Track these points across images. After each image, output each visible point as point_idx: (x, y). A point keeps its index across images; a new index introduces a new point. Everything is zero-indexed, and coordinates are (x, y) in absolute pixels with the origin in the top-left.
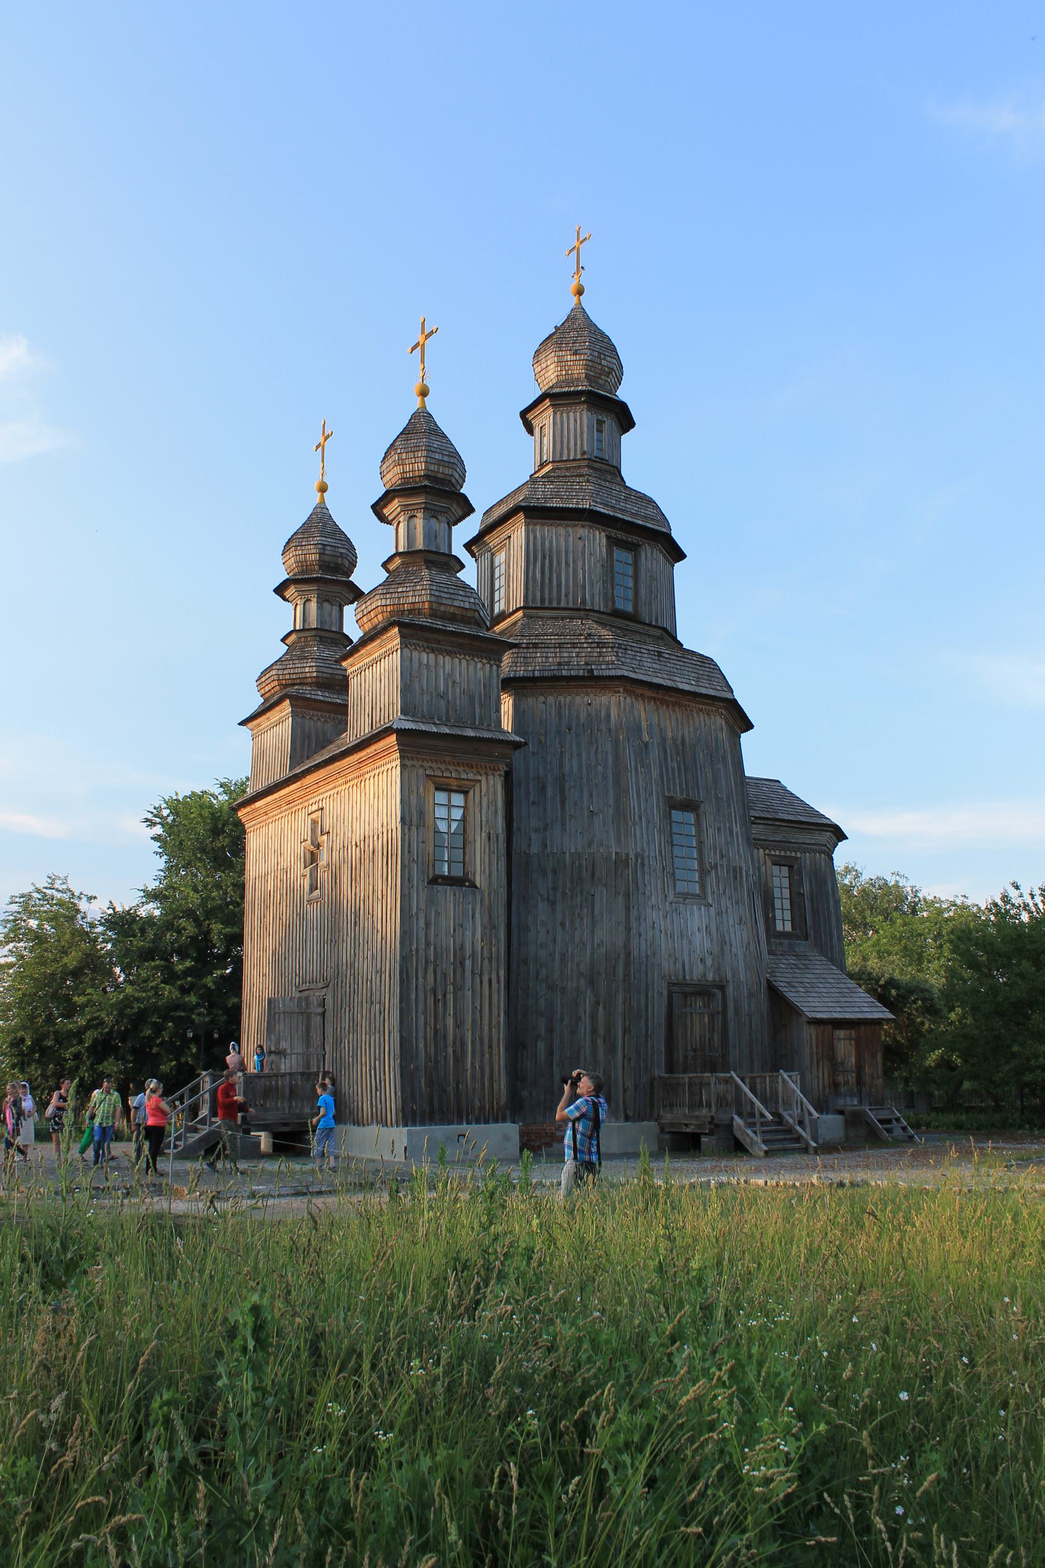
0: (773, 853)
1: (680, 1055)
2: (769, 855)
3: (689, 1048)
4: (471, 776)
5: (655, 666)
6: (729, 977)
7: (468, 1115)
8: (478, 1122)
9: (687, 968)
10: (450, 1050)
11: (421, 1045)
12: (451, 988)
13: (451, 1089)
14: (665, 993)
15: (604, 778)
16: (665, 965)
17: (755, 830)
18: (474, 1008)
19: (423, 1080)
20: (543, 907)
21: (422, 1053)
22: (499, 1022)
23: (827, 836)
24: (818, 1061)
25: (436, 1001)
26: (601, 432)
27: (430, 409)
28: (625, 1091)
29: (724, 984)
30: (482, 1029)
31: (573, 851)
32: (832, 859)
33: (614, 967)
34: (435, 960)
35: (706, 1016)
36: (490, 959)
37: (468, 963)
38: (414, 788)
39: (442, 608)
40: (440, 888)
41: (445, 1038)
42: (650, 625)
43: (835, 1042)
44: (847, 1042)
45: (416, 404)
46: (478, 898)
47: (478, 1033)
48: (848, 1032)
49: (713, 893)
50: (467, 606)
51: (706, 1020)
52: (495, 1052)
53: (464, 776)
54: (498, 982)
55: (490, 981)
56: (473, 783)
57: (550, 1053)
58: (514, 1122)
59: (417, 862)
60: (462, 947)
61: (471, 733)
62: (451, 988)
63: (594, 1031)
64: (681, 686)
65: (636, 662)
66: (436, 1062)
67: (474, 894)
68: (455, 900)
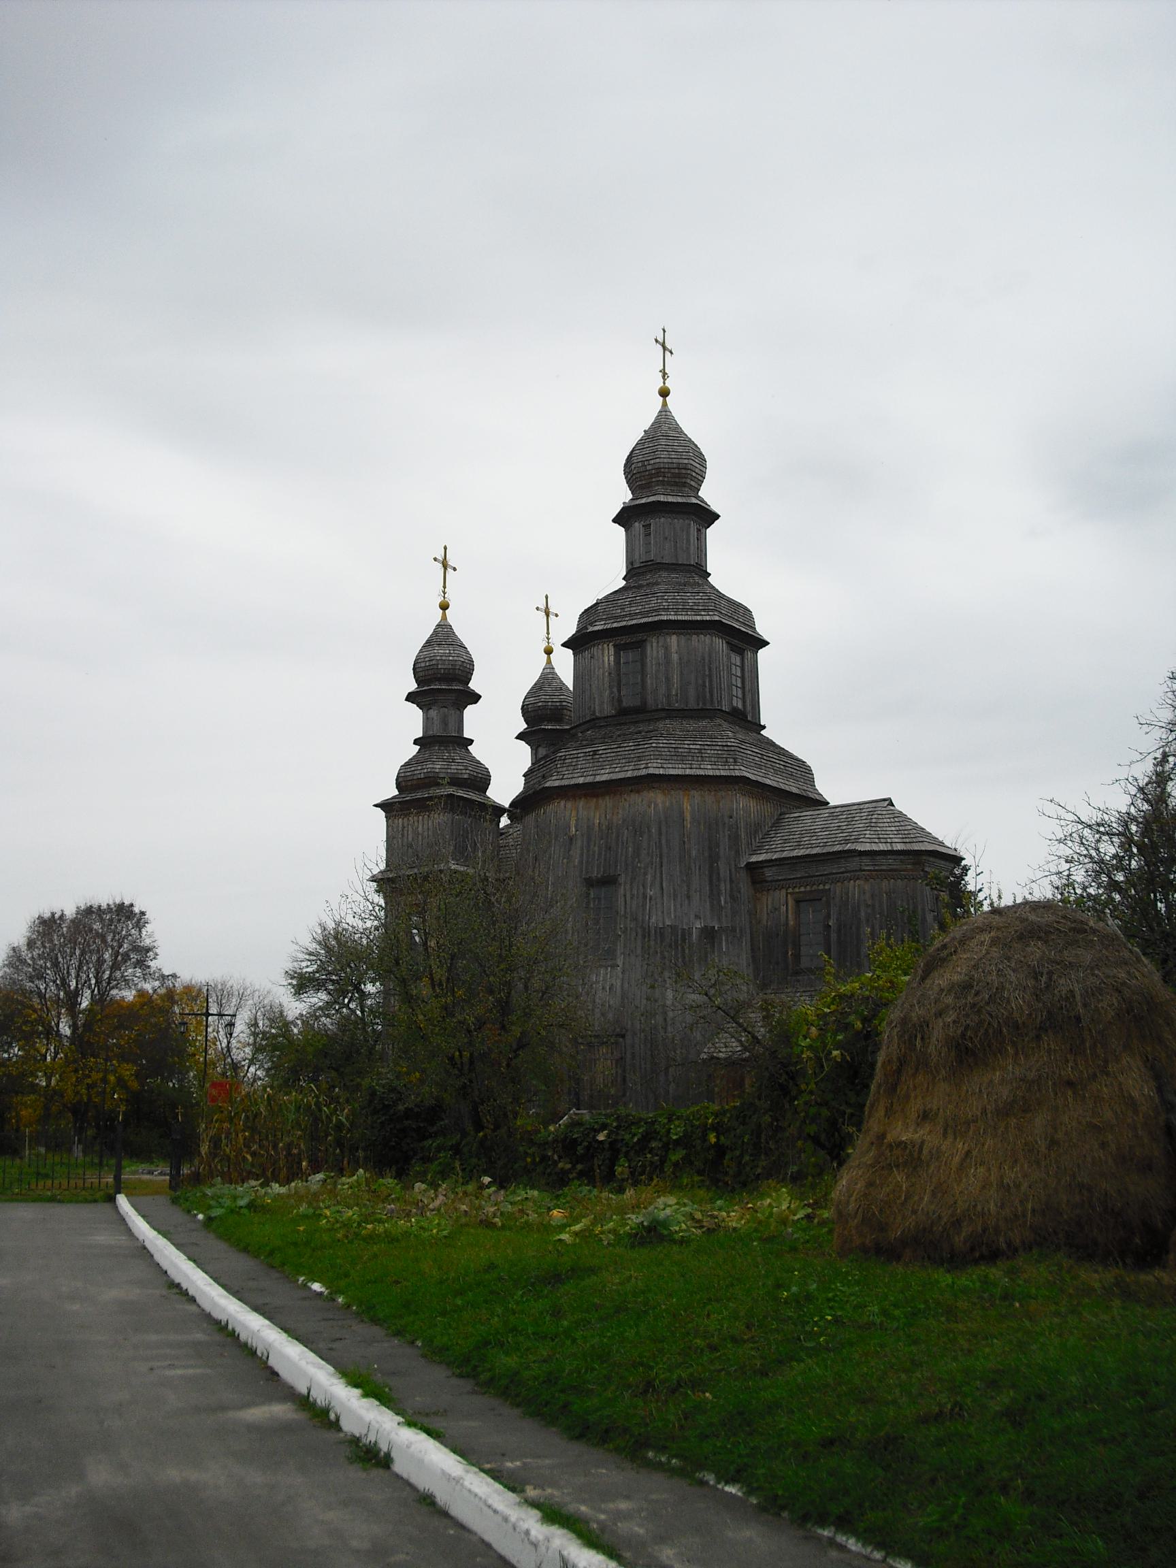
0: (797, 890)
26: (650, 534)
29: (623, 1033)
42: (657, 710)
50: (422, 776)
64: (598, 779)
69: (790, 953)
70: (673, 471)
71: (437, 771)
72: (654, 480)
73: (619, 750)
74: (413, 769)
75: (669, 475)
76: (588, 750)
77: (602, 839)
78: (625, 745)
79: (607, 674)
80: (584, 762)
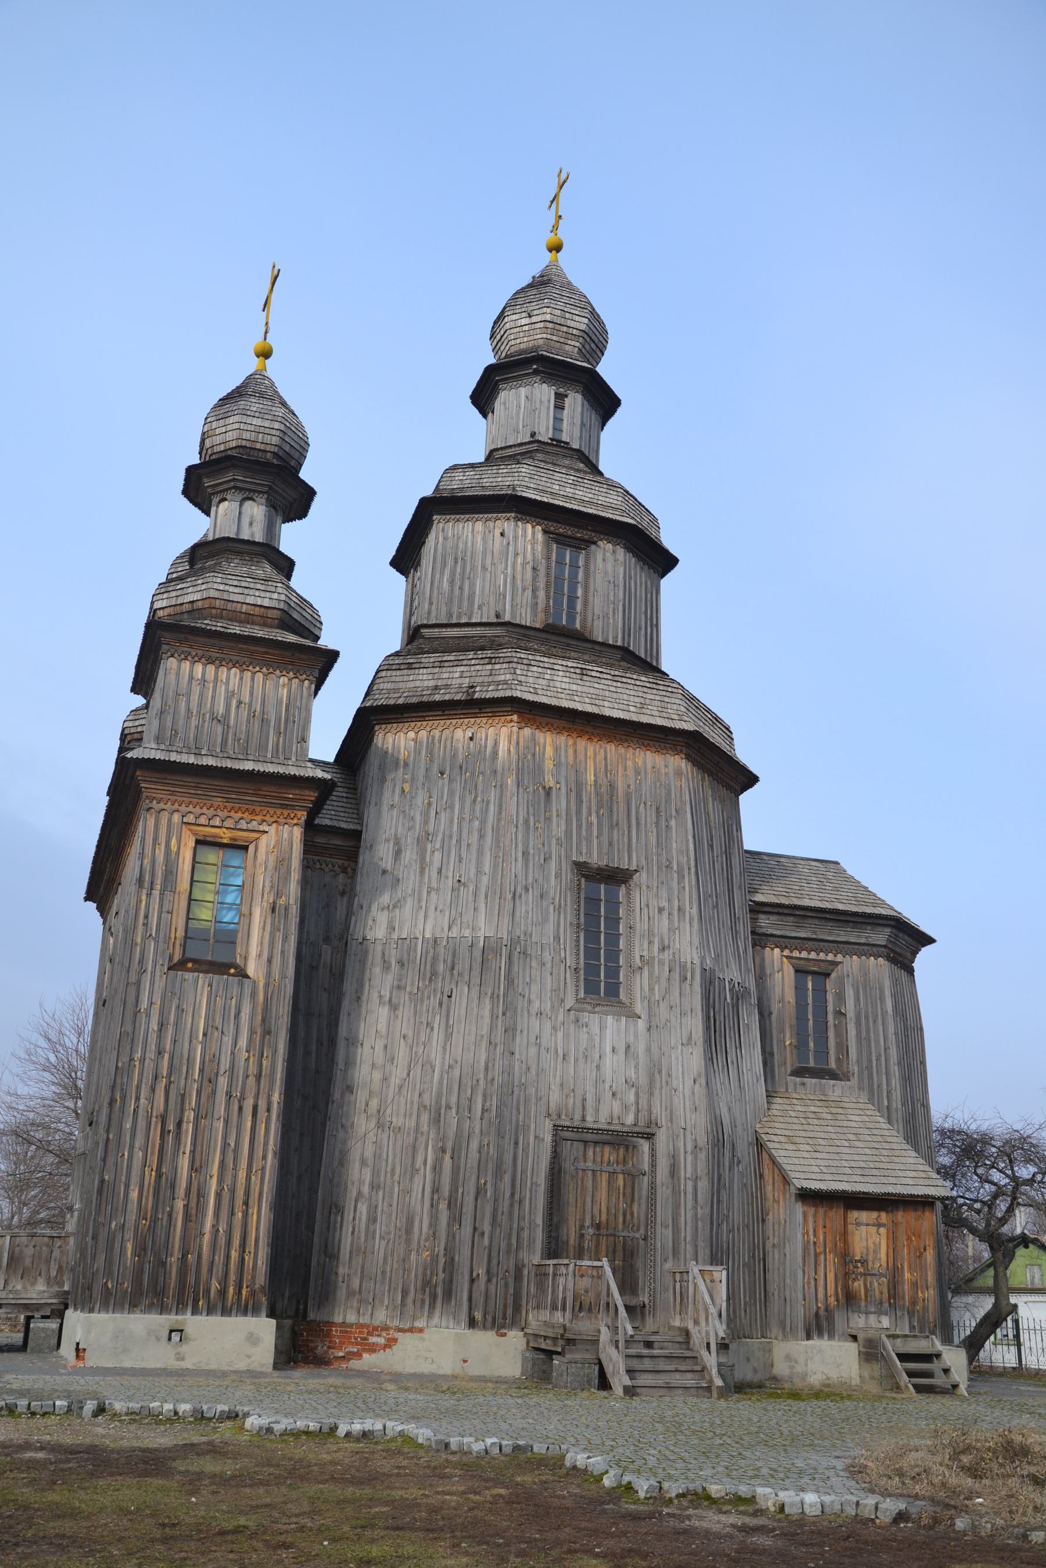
0: (796, 954)
1: (570, 1233)
2: (787, 957)
3: (588, 1223)
4: (254, 825)
5: (574, 687)
6: (663, 1121)
7: (196, 1301)
8: (210, 1311)
9: (590, 1103)
10: (180, 1204)
11: (134, 1195)
12: (190, 1115)
13: (173, 1260)
14: (548, 1138)
15: (482, 837)
16: (555, 1097)
17: (766, 923)
18: (225, 1145)
19: (129, 1246)
20: (384, 1012)
21: (133, 1207)
22: (263, 1169)
23: (881, 937)
24: (816, 1255)
25: (164, 1133)
26: (563, 408)
27: (270, 373)
28: (472, 1281)
30: (235, 1177)
31: (428, 935)
32: (910, 971)
33: (470, 1100)
34: (170, 1075)
35: (621, 1177)
36: (259, 1077)
37: (223, 1082)
38: (163, 840)
39: (229, 606)
40: (189, 976)
41: (173, 1186)
43: (850, 1228)
44: (873, 1229)
45: (253, 363)
46: (247, 991)
47: (228, 1181)
48: (874, 1215)
49: (643, 998)
50: (266, 603)
51: (621, 1182)
52: (254, 1211)
53: (243, 825)
54: (268, 1110)
55: (255, 1108)
56: (255, 835)
57: (372, 1219)
58: (271, 1315)
59: (156, 940)
60: (216, 1059)
61: (248, 766)
62: (190, 1115)
63: (436, 1190)
64: (607, 712)
65: (544, 682)
66: (155, 1220)
67: (241, 985)
68: (210, 993)
69: (788, 1043)
70: (593, 345)
71: (293, 605)
72: (569, 342)
73: (624, 680)
74: (246, 585)
75: (588, 347)
76: (570, 664)
77: (602, 807)
78: (635, 677)
79: (529, 568)
80: (565, 679)
